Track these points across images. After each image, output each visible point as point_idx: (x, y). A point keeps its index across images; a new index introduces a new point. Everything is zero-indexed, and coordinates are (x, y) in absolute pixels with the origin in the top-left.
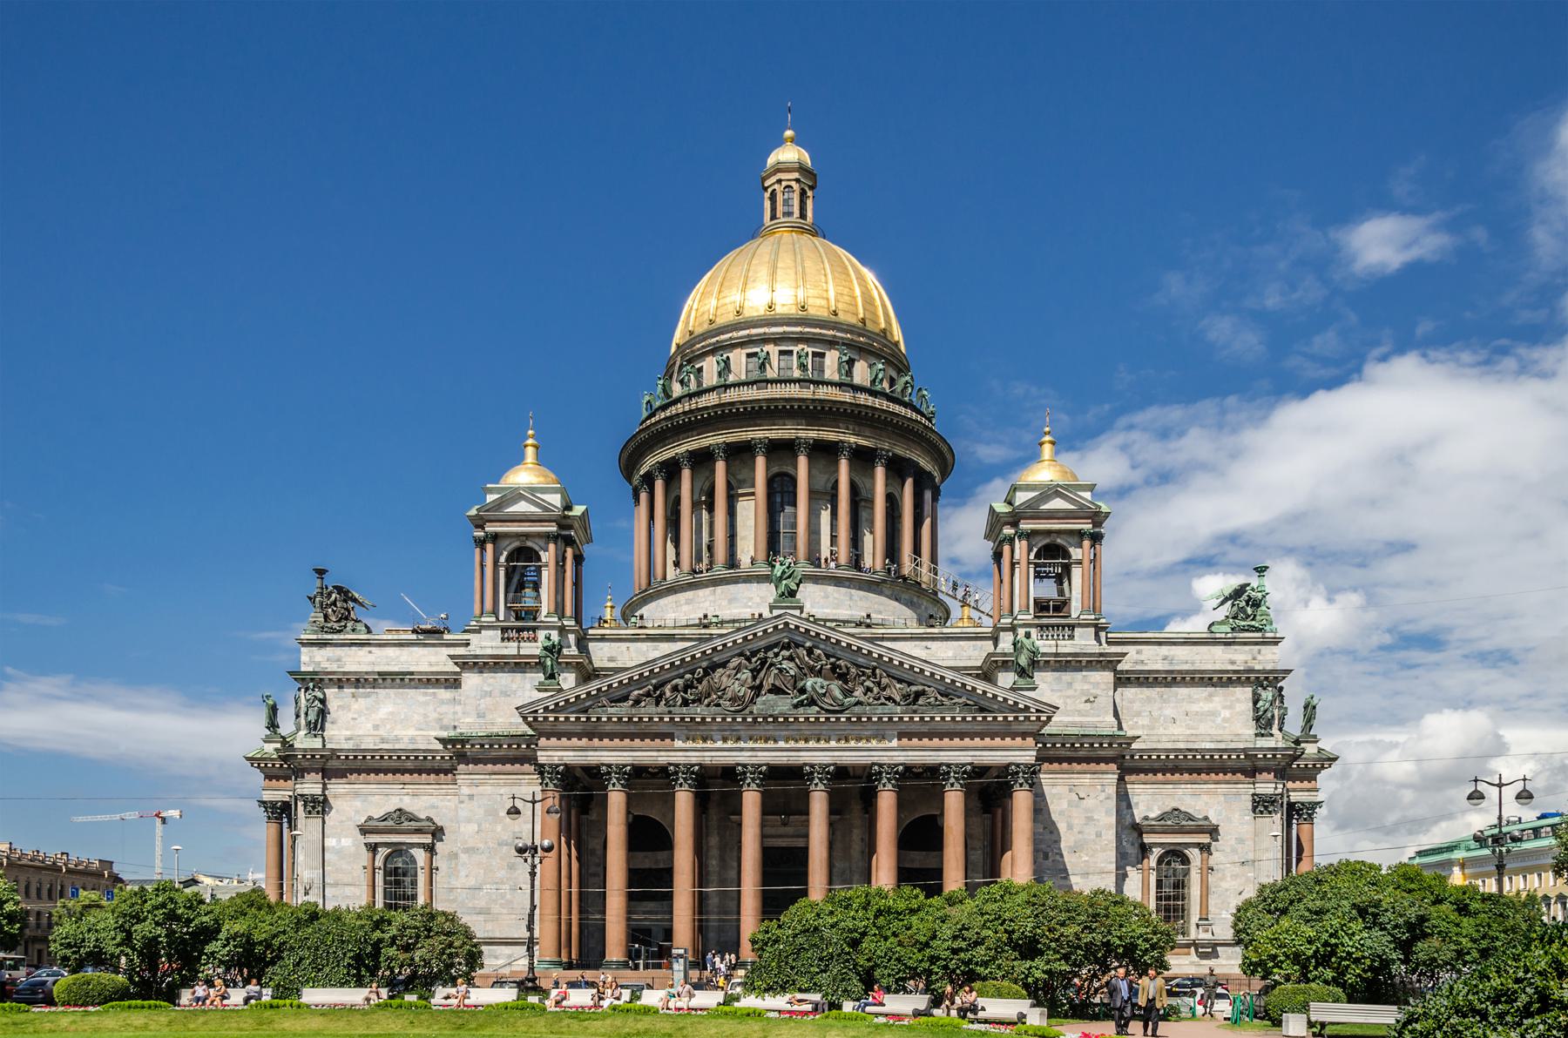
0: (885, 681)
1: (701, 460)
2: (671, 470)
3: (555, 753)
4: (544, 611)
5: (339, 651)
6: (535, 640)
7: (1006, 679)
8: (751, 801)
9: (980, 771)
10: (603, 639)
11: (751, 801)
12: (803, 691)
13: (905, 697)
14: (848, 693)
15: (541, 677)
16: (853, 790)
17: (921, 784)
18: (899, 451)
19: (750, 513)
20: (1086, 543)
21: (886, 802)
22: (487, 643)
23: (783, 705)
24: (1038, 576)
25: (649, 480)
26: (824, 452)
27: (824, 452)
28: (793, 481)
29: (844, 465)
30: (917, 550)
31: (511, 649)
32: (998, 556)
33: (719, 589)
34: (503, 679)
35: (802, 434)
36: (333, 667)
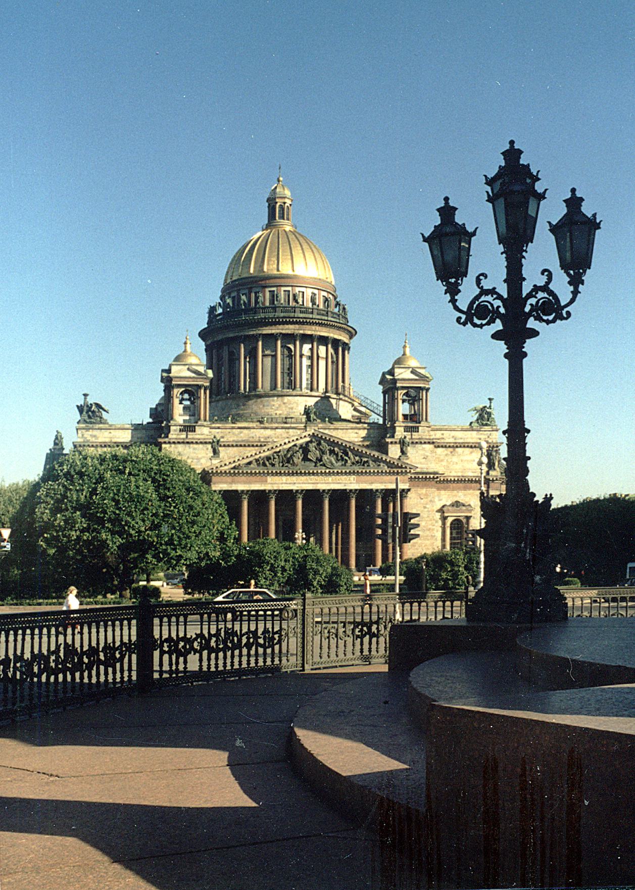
0: (352, 457)
3: (220, 485)
5: (95, 432)
7: (394, 452)
10: (219, 428)
12: (321, 460)
13: (357, 462)
14: (337, 460)
16: (340, 498)
17: (366, 497)
18: (336, 337)
20: (424, 392)
23: (311, 467)
24: (404, 401)
26: (306, 338)
27: (306, 338)
29: (315, 344)
30: (343, 381)
32: (384, 393)
33: (259, 400)
35: (297, 332)
36: (94, 440)
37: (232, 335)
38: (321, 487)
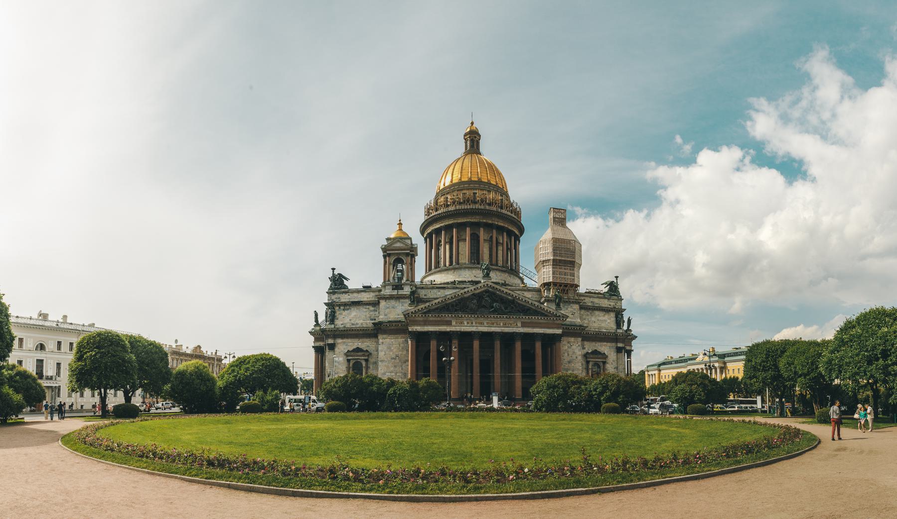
1: (448, 228)
2: (438, 232)
4: (405, 279)
6: (402, 289)
8: (476, 344)
9: (545, 335)
11: (476, 344)
15: (408, 301)
16: (508, 339)
19: (465, 248)
21: (518, 346)
22: (388, 291)
25: (430, 236)
28: (478, 237)
31: (395, 292)
34: (393, 302)
37: (438, 226)
38: (493, 329)
